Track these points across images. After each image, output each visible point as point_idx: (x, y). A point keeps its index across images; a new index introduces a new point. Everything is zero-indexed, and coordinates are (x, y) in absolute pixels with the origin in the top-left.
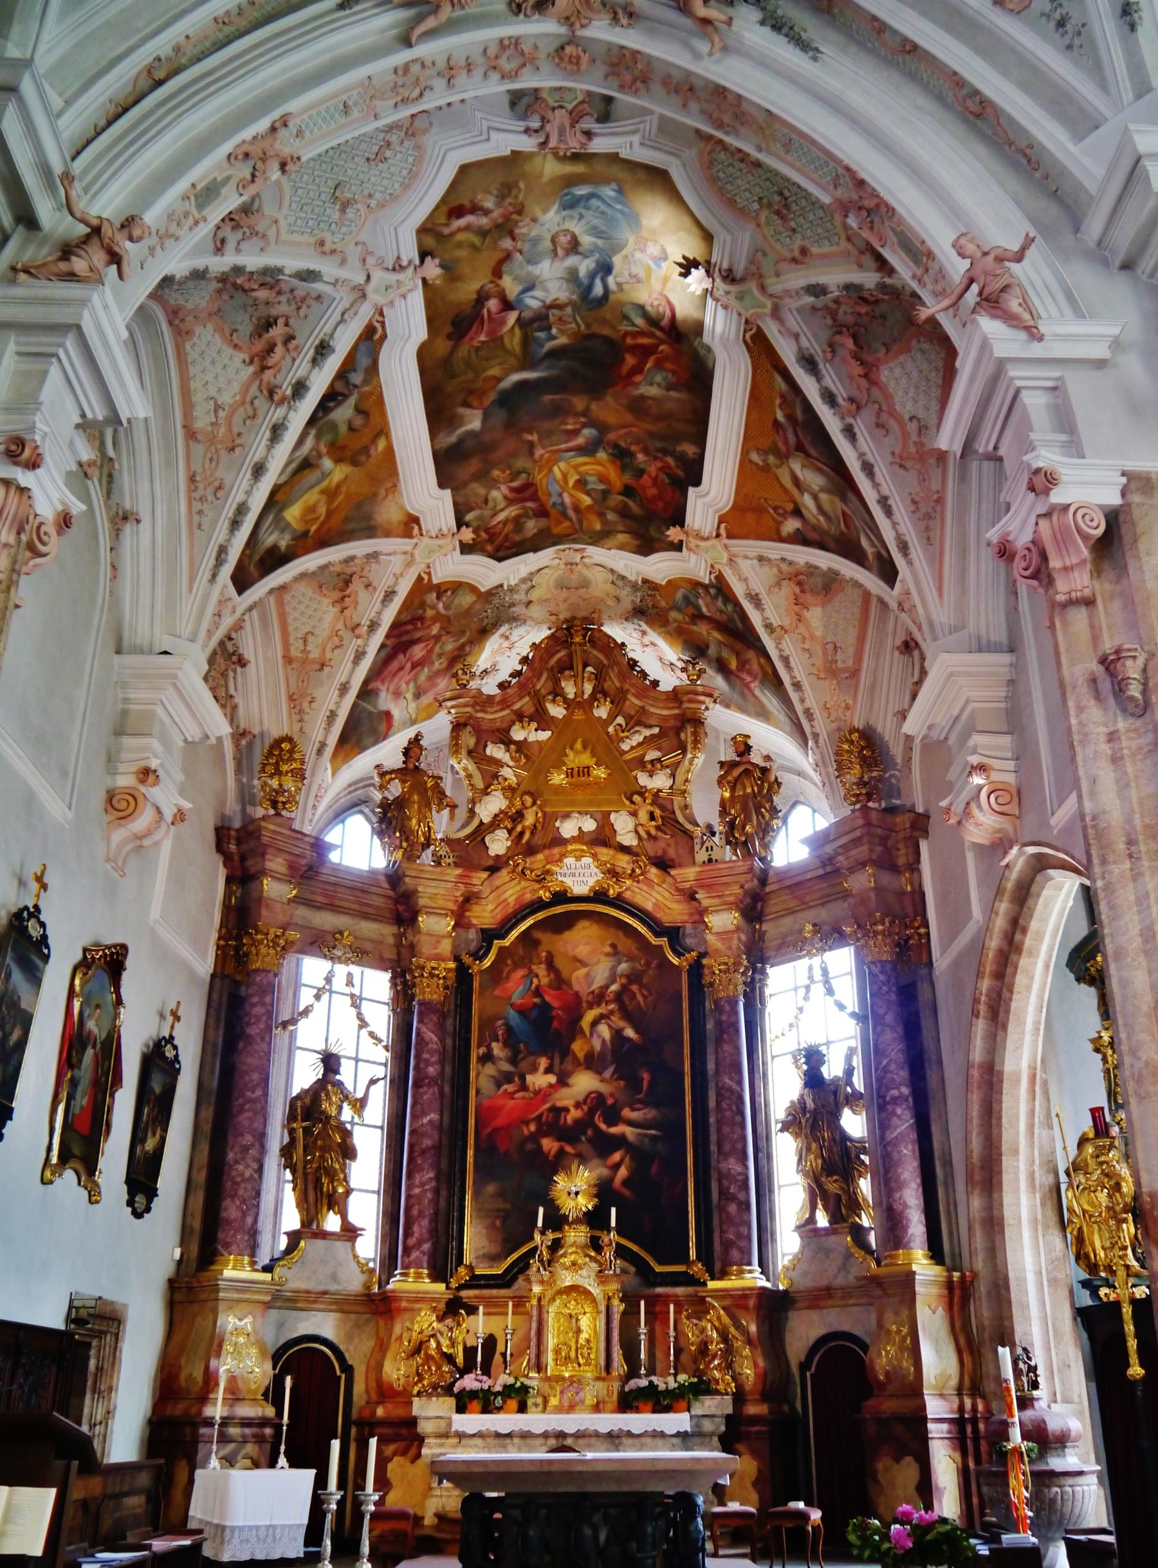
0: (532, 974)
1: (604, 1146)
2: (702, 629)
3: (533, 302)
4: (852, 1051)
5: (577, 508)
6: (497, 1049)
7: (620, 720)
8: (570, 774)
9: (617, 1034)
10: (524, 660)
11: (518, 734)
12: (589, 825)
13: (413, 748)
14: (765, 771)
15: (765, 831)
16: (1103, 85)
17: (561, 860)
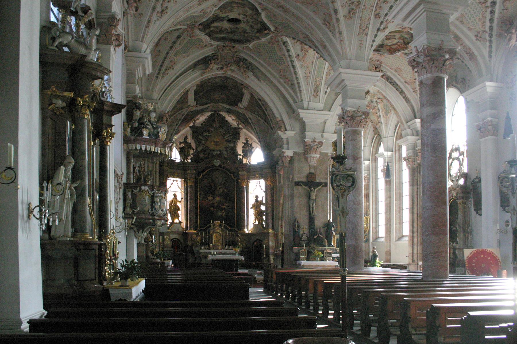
0: (208, 180)
1: (221, 210)
2: (241, 118)
3: (214, 82)
4: (263, 197)
5: (218, 100)
6: (202, 192)
7: (224, 132)
8: (215, 142)
9: (223, 191)
10: (206, 119)
11: (205, 134)
12: (219, 153)
13: (186, 138)
14: (251, 145)
15: (250, 157)
16: (297, 98)
17: (213, 160)
